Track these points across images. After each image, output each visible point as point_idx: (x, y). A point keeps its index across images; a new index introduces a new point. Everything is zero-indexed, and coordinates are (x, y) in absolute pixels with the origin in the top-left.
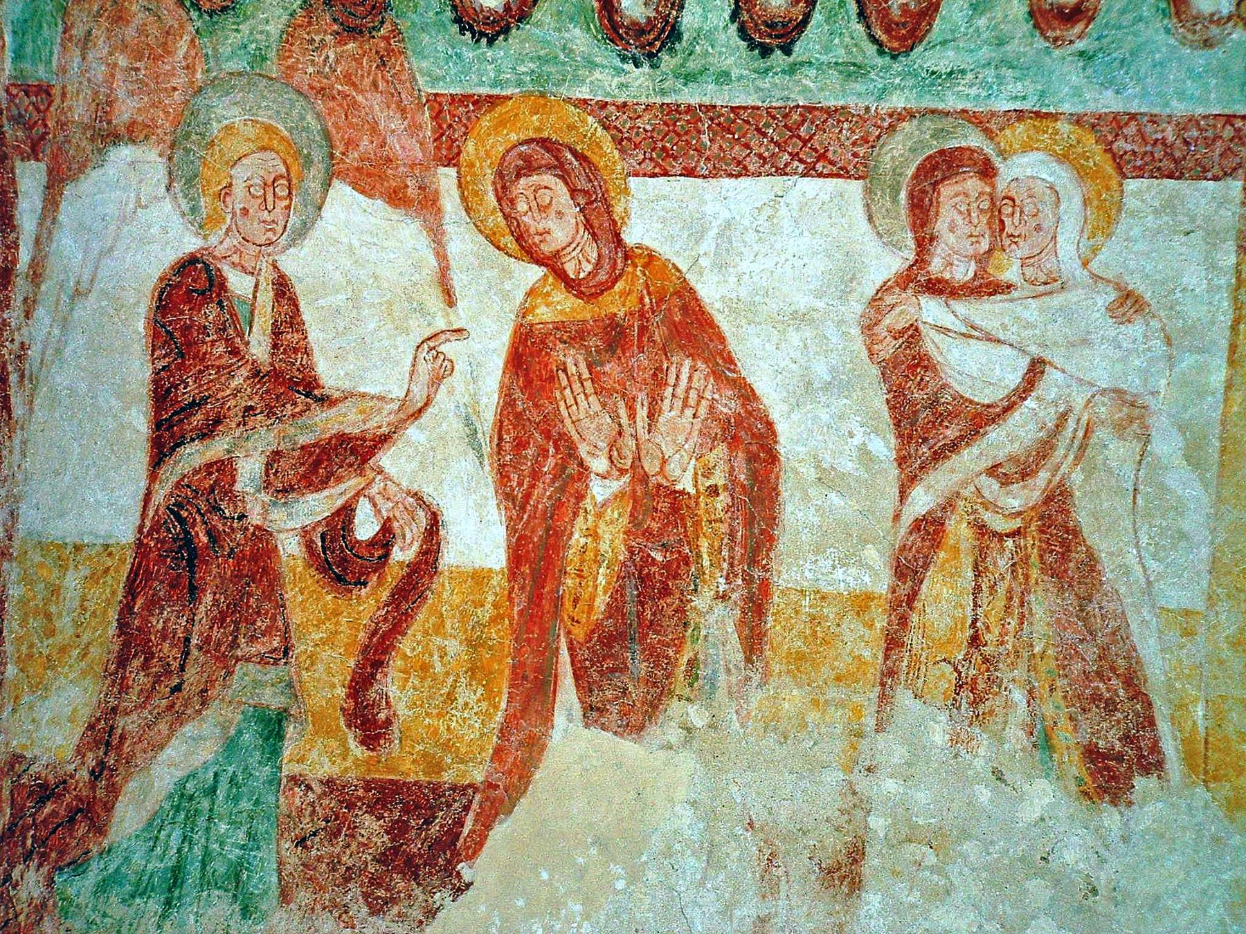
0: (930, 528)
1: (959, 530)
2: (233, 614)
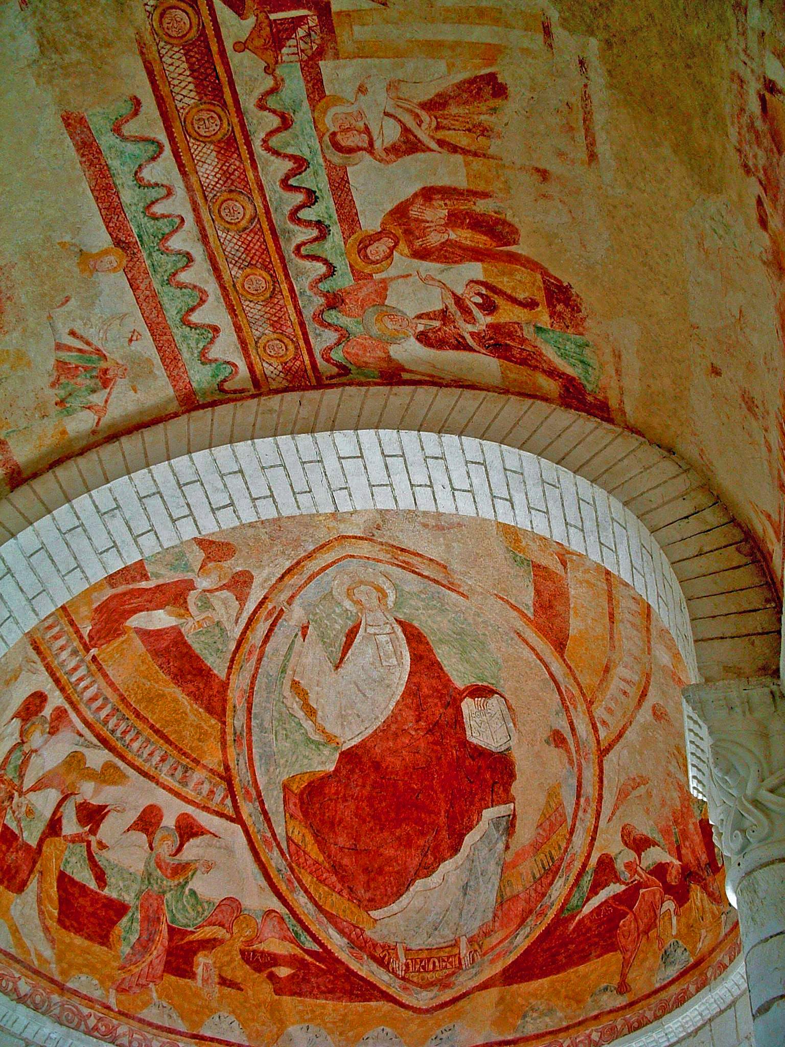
0: (441, 143)
1: (440, 135)
2: (510, 335)
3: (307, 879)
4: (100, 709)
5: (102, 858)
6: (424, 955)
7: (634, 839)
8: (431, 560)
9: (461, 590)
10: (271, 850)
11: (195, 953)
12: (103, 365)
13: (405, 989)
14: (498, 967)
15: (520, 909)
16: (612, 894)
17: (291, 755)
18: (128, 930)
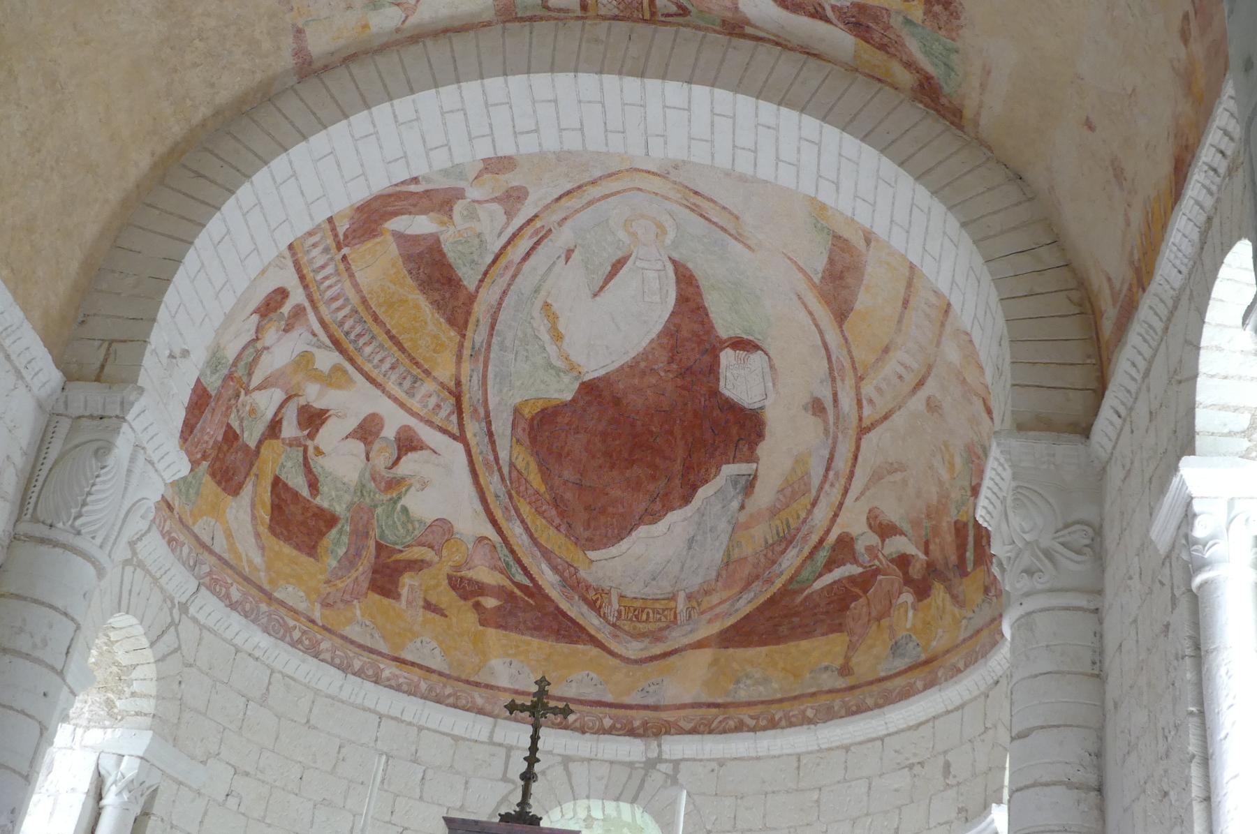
2: (876, 19)
3: (525, 509)
4: (338, 309)
5: (318, 464)
6: (638, 604)
7: (880, 524)
8: (724, 208)
9: (749, 242)
10: (491, 473)
11: (401, 573)
13: (615, 636)
14: (716, 628)
15: (747, 572)
16: (847, 574)
17: (529, 376)
18: (336, 543)
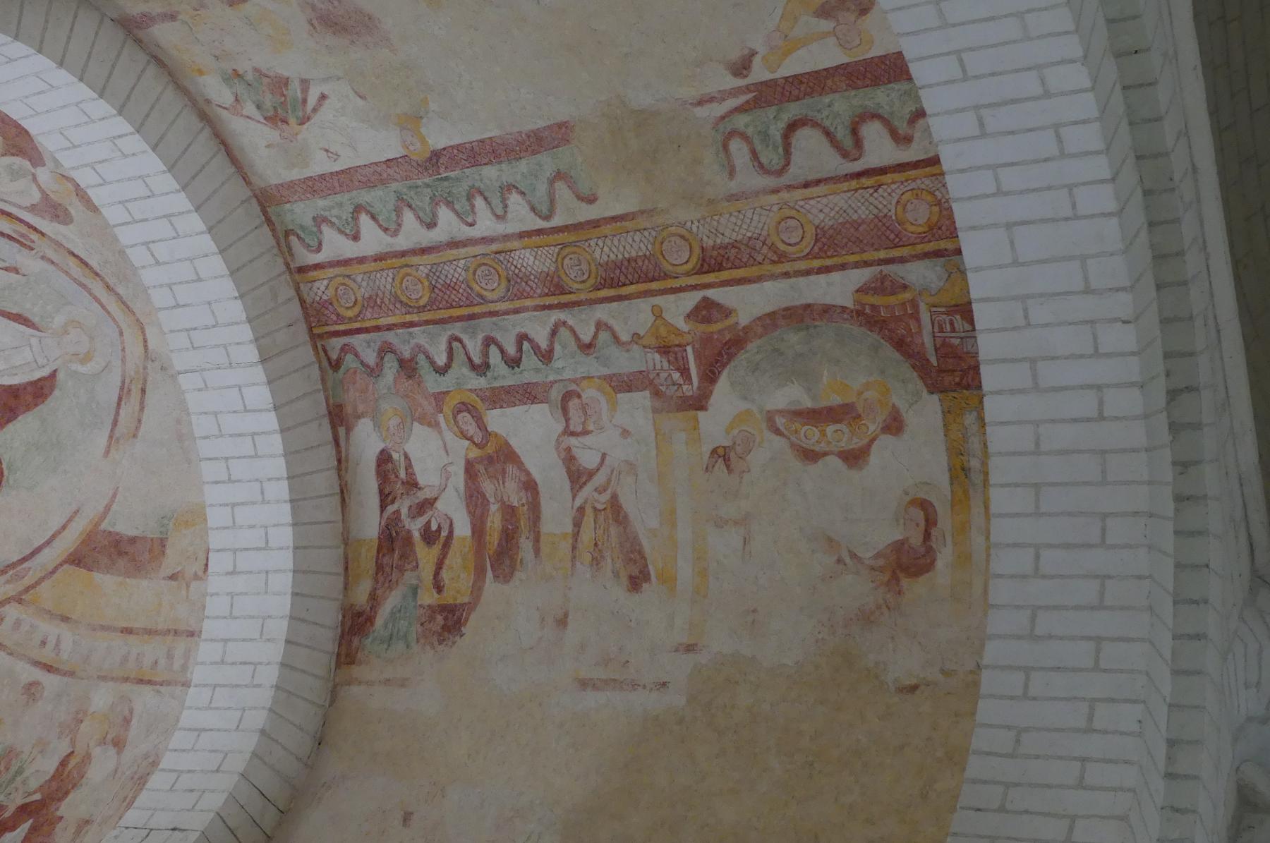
0: (581, 510)
8: (140, 421)
9: (113, 450)
12: (292, 121)
